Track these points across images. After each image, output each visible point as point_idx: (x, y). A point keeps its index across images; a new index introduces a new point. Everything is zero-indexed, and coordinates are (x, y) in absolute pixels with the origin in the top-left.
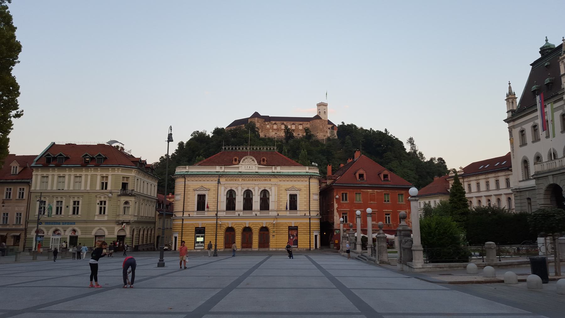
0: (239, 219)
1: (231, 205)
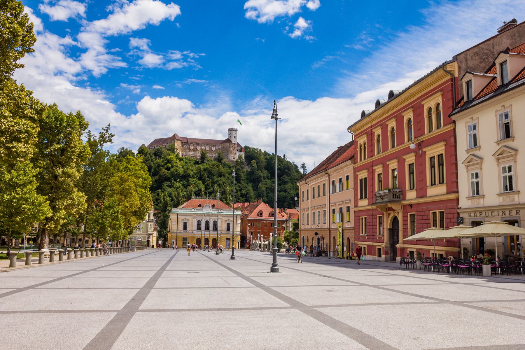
0: (203, 234)
1: (199, 228)
